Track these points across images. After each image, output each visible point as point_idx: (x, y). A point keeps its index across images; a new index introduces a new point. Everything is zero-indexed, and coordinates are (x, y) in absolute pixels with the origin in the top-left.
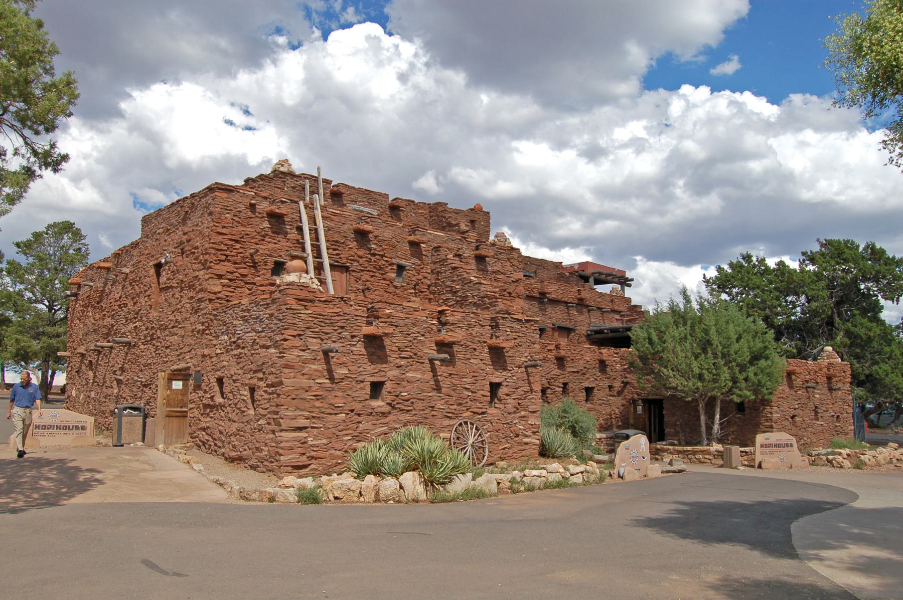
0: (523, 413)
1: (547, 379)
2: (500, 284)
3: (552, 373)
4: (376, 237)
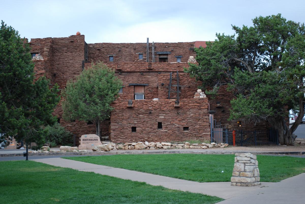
1: (59, 114)
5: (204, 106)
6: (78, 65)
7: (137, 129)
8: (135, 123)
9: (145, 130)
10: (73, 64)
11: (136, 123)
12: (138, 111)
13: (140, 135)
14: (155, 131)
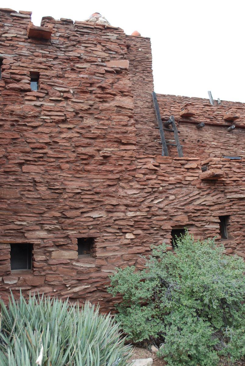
1: (186, 212)
2: (81, 76)
3: (198, 202)
6: (142, 103)
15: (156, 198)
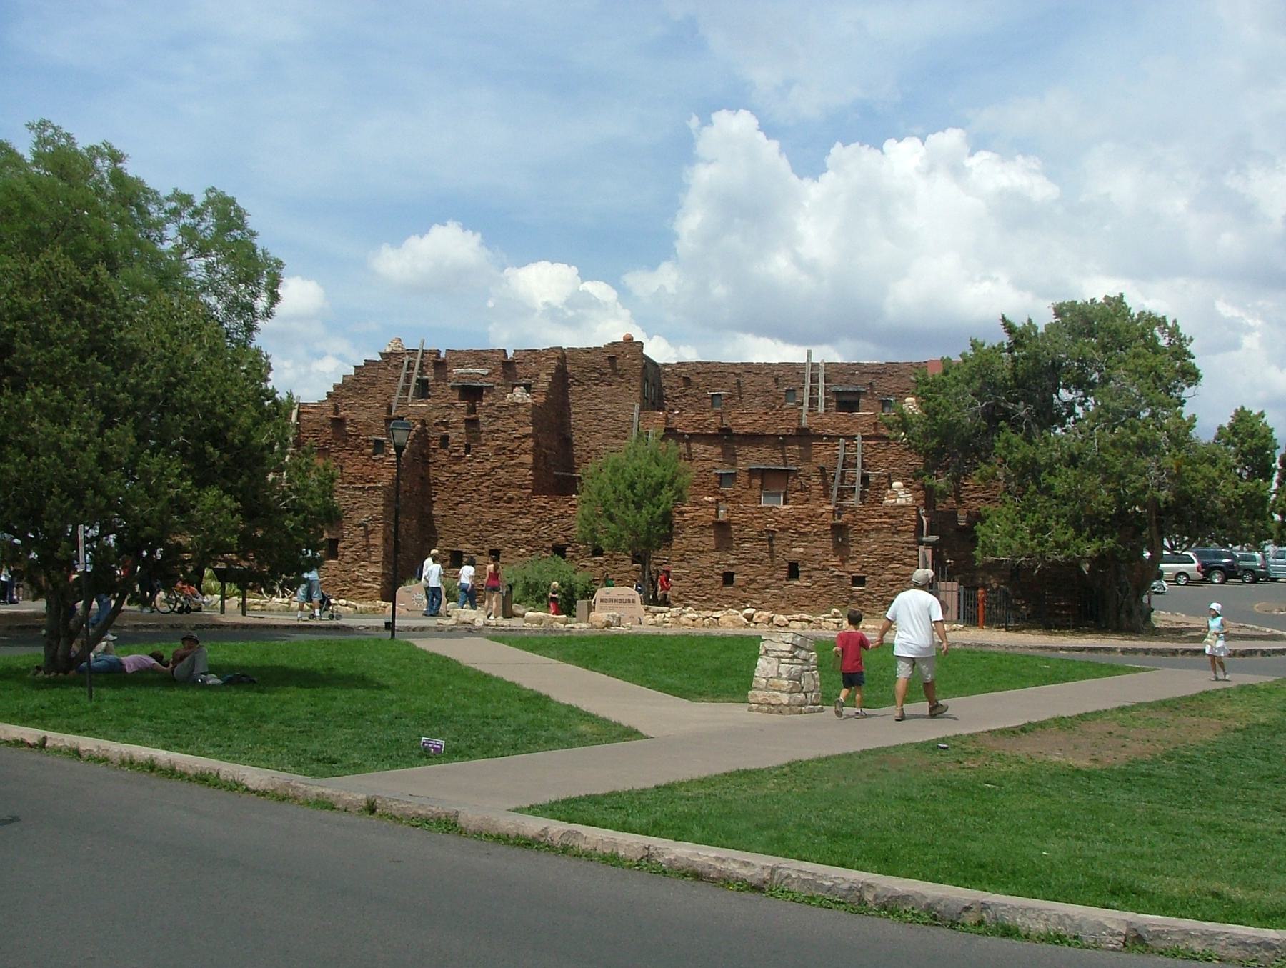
0: (362, 563)
2: (498, 443)
4: (352, 420)
5: (907, 524)
7: (735, 577)
8: (732, 562)
9: (753, 581)
10: (613, 412)
11: (734, 562)
12: (742, 533)
13: (743, 592)
14: (779, 583)
15: (543, 526)
